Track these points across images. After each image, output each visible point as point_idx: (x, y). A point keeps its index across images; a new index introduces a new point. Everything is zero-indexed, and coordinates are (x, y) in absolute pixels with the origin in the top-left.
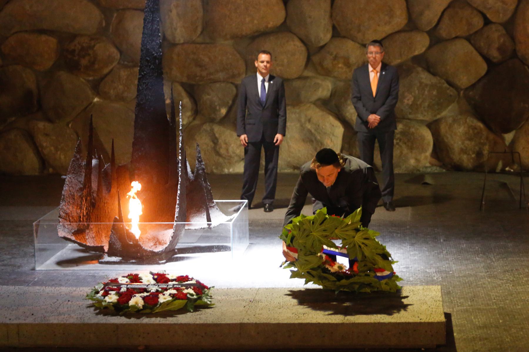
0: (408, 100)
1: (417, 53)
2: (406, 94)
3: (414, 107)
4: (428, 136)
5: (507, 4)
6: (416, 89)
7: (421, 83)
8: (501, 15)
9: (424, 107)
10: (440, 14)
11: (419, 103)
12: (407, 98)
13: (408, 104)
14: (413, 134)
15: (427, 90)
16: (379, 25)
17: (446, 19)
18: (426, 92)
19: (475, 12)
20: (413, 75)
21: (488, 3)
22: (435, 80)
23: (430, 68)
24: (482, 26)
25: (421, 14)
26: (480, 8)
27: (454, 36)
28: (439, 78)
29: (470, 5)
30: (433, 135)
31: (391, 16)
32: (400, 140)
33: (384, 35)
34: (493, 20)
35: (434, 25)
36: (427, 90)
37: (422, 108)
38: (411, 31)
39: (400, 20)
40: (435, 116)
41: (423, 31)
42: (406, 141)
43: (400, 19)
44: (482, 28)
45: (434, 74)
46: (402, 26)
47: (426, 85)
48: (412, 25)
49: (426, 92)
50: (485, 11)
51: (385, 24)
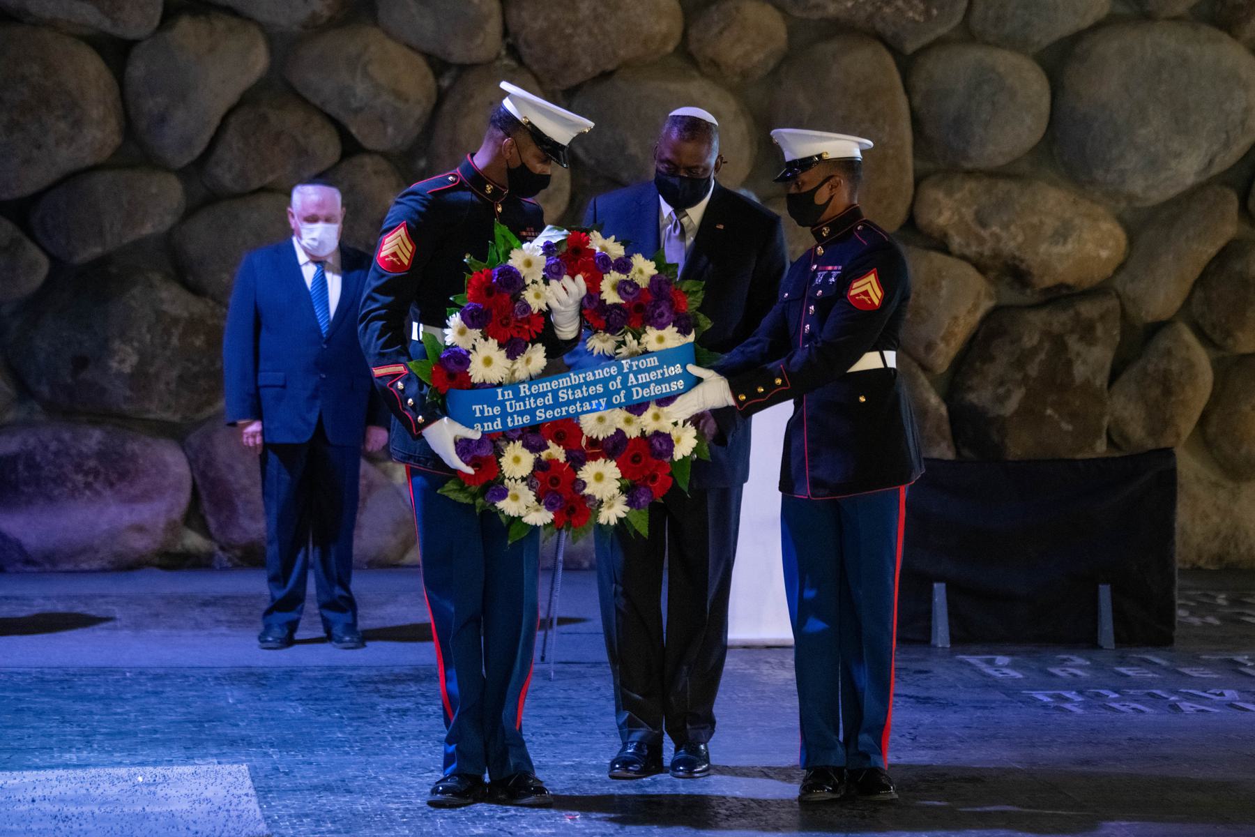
0: (122, 361)
1: (147, 229)
2: (117, 344)
3: (140, 379)
4: (175, 462)
5: (407, 101)
6: (144, 330)
7: (160, 314)
8: (390, 130)
9: (168, 384)
10: (216, 121)
11: (152, 370)
12: (117, 358)
13: (119, 374)
14: (133, 458)
15: (176, 332)
16: (39, 147)
17: (232, 137)
18: (175, 341)
19: (317, 120)
20: (136, 291)
21: (354, 95)
22: (198, 307)
23: (184, 274)
24: (336, 158)
25: (162, 119)
26: (332, 109)
27: (255, 184)
28: (211, 303)
29: (305, 102)
30: (192, 462)
31: (77, 124)
32: (96, 474)
33: (54, 175)
34: (369, 144)
35: (197, 152)
36: (176, 332)
37: (162, 387)
38: (131, 166)
39: (99, 135)
40: (199, 409)
41: (167, 169)
42: (113, 477)
43: (99, 134)
44: (335, 167)
45: (196, 290)
46: (108, 152)
47: (176, 321)
48: (136, 150)
49: (175, 341)
50: (346, 119)
51: (57, 144)
